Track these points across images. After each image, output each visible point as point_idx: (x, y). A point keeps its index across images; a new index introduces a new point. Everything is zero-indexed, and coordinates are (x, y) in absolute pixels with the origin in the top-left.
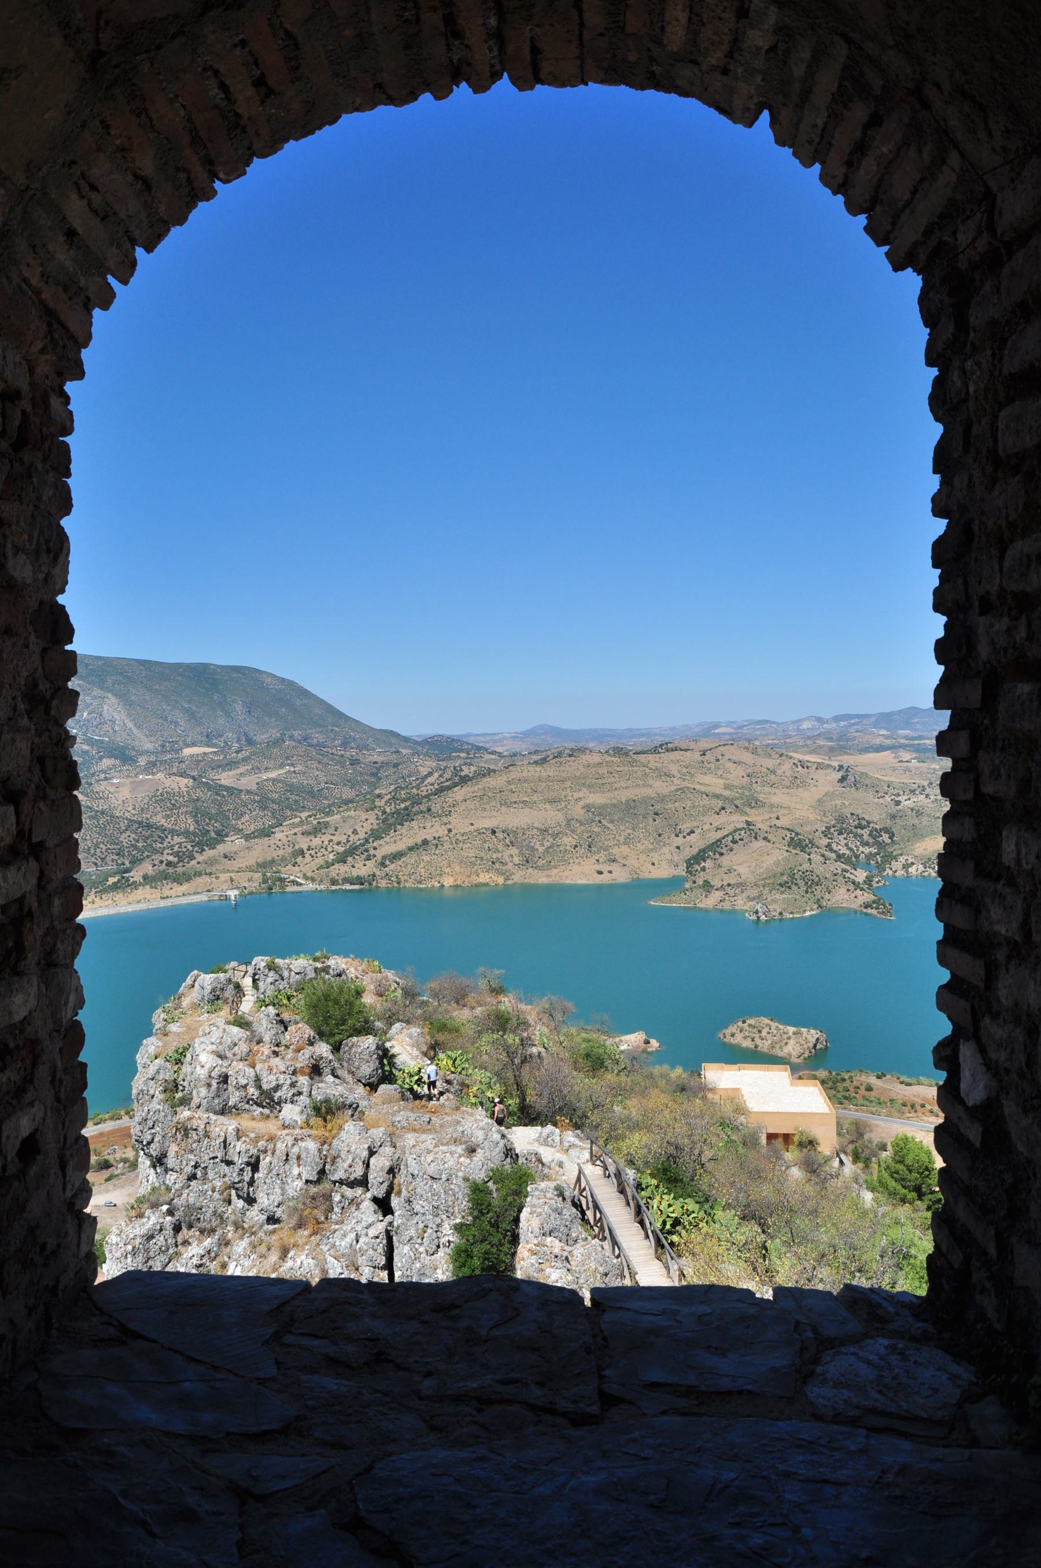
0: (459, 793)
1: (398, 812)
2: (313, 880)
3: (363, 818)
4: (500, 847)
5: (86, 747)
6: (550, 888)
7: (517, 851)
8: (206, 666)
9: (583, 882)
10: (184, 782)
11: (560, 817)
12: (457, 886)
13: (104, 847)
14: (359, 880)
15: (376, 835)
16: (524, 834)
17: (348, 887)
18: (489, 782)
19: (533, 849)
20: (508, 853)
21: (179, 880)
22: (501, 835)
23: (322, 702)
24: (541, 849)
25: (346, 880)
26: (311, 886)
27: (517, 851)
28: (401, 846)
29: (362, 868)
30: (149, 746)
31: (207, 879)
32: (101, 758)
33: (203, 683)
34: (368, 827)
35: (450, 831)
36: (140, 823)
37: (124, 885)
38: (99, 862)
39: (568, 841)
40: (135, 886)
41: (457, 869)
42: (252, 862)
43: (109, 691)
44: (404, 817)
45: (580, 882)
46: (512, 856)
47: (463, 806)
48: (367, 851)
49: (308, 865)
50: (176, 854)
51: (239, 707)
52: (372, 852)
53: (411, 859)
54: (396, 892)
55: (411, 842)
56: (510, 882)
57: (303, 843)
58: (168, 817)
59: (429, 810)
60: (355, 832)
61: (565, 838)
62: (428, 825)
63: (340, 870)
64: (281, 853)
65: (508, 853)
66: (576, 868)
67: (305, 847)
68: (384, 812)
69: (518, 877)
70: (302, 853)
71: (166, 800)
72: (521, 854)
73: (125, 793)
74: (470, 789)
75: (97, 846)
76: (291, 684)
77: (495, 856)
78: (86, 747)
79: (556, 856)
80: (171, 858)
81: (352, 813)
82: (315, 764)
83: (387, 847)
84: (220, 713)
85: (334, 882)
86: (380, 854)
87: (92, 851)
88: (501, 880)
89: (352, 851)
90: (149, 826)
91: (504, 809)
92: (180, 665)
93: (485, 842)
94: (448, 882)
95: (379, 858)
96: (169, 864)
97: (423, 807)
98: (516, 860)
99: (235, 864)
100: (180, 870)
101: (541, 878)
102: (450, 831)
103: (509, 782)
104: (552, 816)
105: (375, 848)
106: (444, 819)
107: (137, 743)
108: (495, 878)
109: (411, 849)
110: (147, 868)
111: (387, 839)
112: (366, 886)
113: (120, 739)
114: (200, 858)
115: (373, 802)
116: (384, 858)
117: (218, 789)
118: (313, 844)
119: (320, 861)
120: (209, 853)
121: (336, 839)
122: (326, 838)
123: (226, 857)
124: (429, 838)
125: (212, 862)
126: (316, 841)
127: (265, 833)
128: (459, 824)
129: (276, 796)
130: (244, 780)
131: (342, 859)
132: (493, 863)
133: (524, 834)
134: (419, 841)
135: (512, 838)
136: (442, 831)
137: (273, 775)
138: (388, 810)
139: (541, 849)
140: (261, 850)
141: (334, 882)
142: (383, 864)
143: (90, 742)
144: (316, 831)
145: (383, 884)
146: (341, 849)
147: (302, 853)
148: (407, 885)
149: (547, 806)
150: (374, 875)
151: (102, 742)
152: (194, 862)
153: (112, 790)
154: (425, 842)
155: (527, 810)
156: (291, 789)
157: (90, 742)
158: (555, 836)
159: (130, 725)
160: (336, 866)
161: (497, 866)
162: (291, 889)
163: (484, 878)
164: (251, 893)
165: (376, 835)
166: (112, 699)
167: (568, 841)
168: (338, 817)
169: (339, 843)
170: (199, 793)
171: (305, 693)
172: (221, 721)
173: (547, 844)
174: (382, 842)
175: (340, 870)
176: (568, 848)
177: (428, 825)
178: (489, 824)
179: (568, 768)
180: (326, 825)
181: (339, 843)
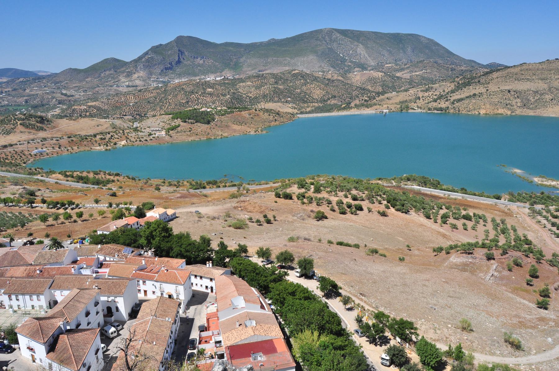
0: (495, 75)
1: (464, 83)
2: (421, 108)
3: (449, 86)
4: (511, 98)
5: (350, 64)
6: (534, 117)
7: (520, 101)
8: (398, 34)
9: (554, 116)
10: (380, 74)
11: (546, 86)
12: (486, 114)
14: (441, 109)
15: (453, 92)
16: (525, 93)
17: (436, 112)
18: (512, 70)
19: (529, 100)
20: (515, 101)
21: (367, 107)
22: (513, 93)
23: (444, 48)
24: (533, 100)
25: (435, 109)
26: (419, 110)
27: (520, 101)
28: (463, 96)
29: (443, 104)
30: (373, 64)
31: (378, 106)
32: (355, 68)
33: (397, 40)
34: (450, 89)
35: (487, 90)
36: (361, 88)
37: (348, 107)
38: (343, 101)
39: (548, 97)
40: (351, 108)
41: (488, 106)
42: (398, 101)
43: (360, 43)
44: (467, 84)
45: (551, 116)
46: (517, 102)
47: (496, 80)
48: (447, 97)
49: (420, 103)
50: (369, 97)
51: (409, 49)
52: (449, 98)
53: (466, 102)
54: (458, 114)
55: (468, 95)
56: (514, 114)
57: (421, 94)
58: (372, 86)
59: (479, 82)
60: (444, 91)
61: (547, 96)
62: (477, 88)
63: (435, 104)
64: (410, 98)
65: (515, 101)
66: (550, 109)
67: (421, 96)
68: (459, 83)
69: (519, 112)
70: (419, 98)
71: (372, 80)
72: (522, 101)
73: (358, 78)
74: (501, 73)
75: (343, 95)
76: (432, 41)
77: (508, 102)
78: (350, 64)
79: (541, 103)
80: (366, 98)
81: (444, 83)
82: (436, 70)
83: (456, 96)
84: (401, 51)
85: (429, 109)
86: (452, 99)
88: (509, 113)
89: (440, 97)
90: (364, 89)
91: (516, 82)
92: (388, 34)
93: (504, 95)
94: (482, 112)
95: (452, 100)
96: (365, 101)
97: (476, 80)
98: (519, 104)
99: (391, 102)
101: (531, 113)
102: (487, 90)
103: (521, 70)
104: (541, 86)
105: (451, 97)
106: (486, 86)
107: (368, 63)
108: (506, 112)
109: (467, 97)
110: (357, 102)
111: (457, 93)
112: (444, 112)
113: (362, 61)
114: (377, 99)
115: (454, 79)
116: (454, 100)
117: (393, 77)
118: (425, 95)
119: (427, 101)
120: (381, 97)
121: (435, 94)
122: (430, 93)
123: (387, 98)
124: (477, 93)
125: (382, 100)
127: (406, 91)
128: (492, 87)
129: (417, 81)
130: (405, 75)
131: (435, 101)
132: (507, 105)
133: (525, 93)
134: (472, 94)
135: (518, 94)
136: (483, 90)
137: (417, 73)
138: (460, 82)
139: (533, 100)
140: (403, 96)
141: (429, 109)
142: (453, 103)
143: (351, 62)
144: (427, 90)
145: (452, 111)
146: (436, 97)
147: (419, 98)
148: (463, 112)
149: (540, 81)
150: (448, 107)
151: (356, 62)
152: (375, 100)
153: (353, 76)
154: (475, 95)
155: (528, 83)
156: (424, 78)
157: (351, 62)
158: (542, 94)
159: (366, 55)
160: (432, 103)
161: (508, 106)
162: (410, 111)
163: (501, 111)
164: (393, 112)
165: (453, 92)
166: (361, 46)
167: (548, 97)
168: (437, 85)
169: (436, 95)
170: (386, 78)
171: (438, 44)
172: (401, 55)
173: (536, 98)
174: (454, 94)
175: (435, 104)
176: (548, 100)
177: (477, 88)
178: (508, 88)
179: (554, 65)
180: (432, 88)
181: (436, 95)
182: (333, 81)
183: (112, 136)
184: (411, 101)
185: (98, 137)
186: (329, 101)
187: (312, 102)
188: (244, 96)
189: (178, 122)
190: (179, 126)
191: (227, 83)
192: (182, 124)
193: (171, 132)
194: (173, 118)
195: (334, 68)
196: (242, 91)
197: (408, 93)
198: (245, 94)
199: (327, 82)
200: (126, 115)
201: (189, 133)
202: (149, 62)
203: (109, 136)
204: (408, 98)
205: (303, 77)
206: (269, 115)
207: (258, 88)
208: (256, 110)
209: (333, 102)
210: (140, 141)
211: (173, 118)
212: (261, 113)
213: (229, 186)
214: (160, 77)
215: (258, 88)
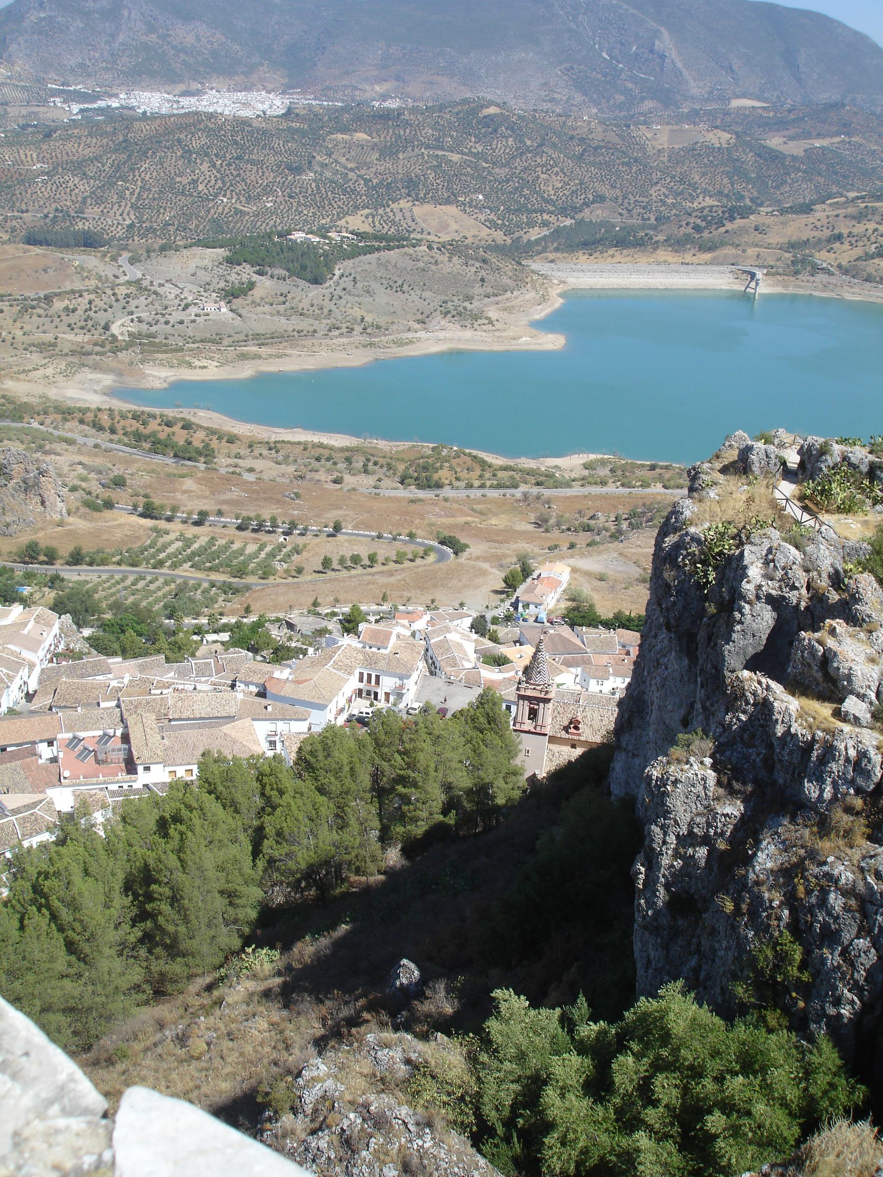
5: (630, 85)
10: (726, 136)
13: (633, 199)
32: (643, 99)
38: (624, 212)
40: (656, 246)
42: (784, 240)
58: (704, 174)
67: (845, 232)
70: (839, 238)
78: (630, 85)
87: (620, 201)
96: (697, 228)
100: (706, 234)
118: (855, 231)
119: (858, 251)
120: (739, 222)
122: (871, 226)
126: (859, 228)
127: (806, 209)
144: (860, 217)
147: (839, 238)
153: (649, 136)
160: (876, 261)
182: (596, 149)
183: (90, 303)
184: (818, 244)
185: (59, 305)
186: (587, 211)
187: (542, 212)
188: (351, 175)
189: (247, 272)
190: (252, 285)
191: (297, 130)
192: (255, 278)
193: (237, 302)
194: (230, 261)
195: (585, 94)
196: (343, 160)
197: (811, 219)
198: (352, 170)
199: (579, 149)
200: (27, 211)
201: (282, 308)
202: (40, 33)
203: (82, 303)
204: (808, 234)
205: (512, 130)
206: (467, 265)
207: (388, 152)
208: (430, 248)
209: (596, 214)
210: (167, 323)
211: (230, 261)
212: (444, 258)
213: (491, 487)
214: (71, 79)
215: (388, 152)
